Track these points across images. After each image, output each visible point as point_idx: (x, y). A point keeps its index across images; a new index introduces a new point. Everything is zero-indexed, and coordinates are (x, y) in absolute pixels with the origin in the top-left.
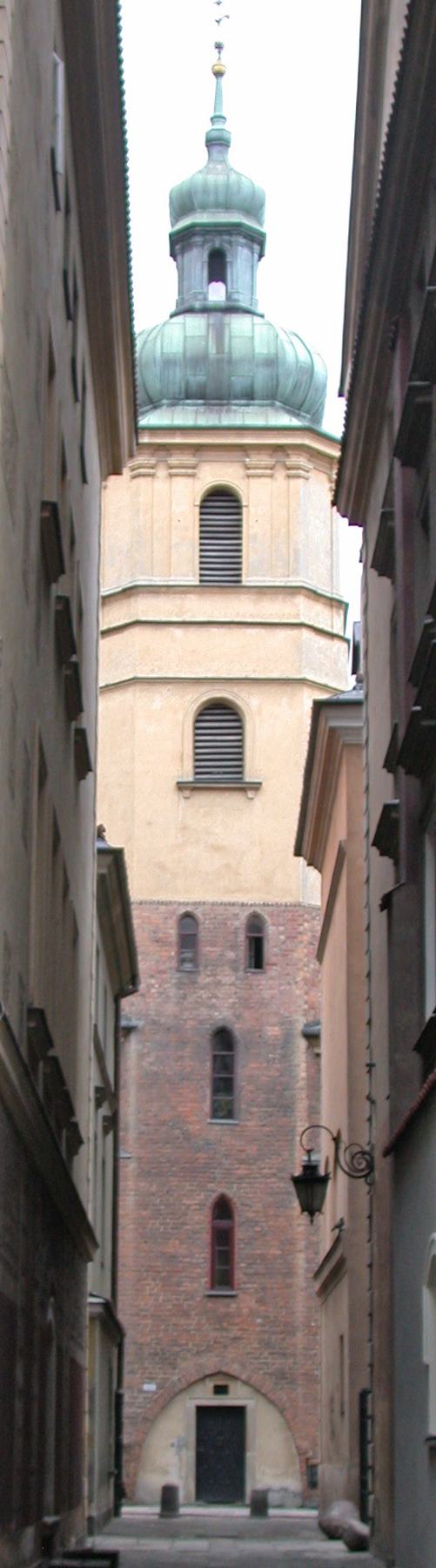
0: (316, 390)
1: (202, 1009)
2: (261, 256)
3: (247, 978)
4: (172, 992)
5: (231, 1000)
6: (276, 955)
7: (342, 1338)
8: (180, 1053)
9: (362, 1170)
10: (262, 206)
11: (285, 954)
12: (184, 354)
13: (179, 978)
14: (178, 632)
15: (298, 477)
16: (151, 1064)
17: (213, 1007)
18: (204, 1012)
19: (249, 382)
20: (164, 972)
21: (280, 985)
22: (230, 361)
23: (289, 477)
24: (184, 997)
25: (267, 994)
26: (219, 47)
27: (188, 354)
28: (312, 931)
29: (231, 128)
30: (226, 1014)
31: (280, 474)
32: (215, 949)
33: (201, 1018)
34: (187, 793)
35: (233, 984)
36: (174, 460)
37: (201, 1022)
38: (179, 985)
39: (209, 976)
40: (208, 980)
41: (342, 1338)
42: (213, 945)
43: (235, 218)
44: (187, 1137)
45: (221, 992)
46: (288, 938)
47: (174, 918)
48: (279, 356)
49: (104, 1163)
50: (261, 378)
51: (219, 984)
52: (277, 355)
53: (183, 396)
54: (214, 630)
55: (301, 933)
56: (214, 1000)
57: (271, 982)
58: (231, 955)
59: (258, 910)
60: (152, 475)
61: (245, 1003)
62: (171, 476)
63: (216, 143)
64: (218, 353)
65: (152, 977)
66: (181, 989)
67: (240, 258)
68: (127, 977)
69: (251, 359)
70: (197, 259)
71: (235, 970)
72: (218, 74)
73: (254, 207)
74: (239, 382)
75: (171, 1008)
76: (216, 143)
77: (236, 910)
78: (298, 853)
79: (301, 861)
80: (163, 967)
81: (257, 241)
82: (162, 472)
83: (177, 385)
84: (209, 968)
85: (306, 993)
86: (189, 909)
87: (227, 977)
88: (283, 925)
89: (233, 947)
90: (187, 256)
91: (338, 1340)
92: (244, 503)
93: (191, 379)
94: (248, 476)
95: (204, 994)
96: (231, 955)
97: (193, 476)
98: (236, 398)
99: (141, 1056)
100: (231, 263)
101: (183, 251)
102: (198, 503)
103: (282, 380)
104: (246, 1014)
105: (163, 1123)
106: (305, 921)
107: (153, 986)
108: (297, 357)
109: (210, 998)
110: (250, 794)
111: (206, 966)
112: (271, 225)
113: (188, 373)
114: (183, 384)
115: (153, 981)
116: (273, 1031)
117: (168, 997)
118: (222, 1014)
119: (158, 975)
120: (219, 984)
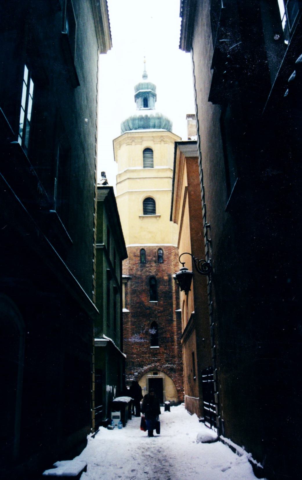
1: (147, 273)
2: (156, 101)
3: (158, 264)
4: (139, 269)
5: (155, 270)
6: (166, 258)
7: (193, 354)
8: (142, 285)
9: (206, 271)
10: (155, 89)
11: (168, 258)
13: (141, 265)
14: (138, 180)
15: (167, 143)
16: (134, 287)
17: (150, 272)
18: (148, 273)
20: (137, 264)
21: (167, 266)
23: (165, 143)
24: (142, 270)
25: (164, 268)
26: (145, 57)
28: (175, 252)
29: (148, 73)
30: (153, 274)
31: (163, 143)
32: (150, 257)
33: (147, 275)
34: (142, 219)
35: (155, 266)
36: (136, 141)
37: (147, 276)
38: (141, 267)
39: (148, 264)
40: (149, 265)
41: (193, 354)
42: (150, 256)
43: (150, 90)
44: (144, 306)
45: (152, 269)
46: (168, 254)
47: (139, 250)
51: (151, 266)
54: (147, 179)
55: (172, 253)
56: (150, 270)
57: (165, 265)
58: (154, 259)
59: (161, 247)
60: (131, 144)
61: (158, 271)
62: (136, 144)
65: (134, 265)
66: (141, 268)
67: (151, 101)
69: (154, 118)
70: (140, 101)
71: (155, 262)
72: (145, 63)
73: (154, 88)
75: (139, 273)
76: (145, 76)
77: (156, 247)
78: (171, 220)
79: (172, 222)
80: (137, 262)
81: (154, 95)
82: (133, 143)
84: (149, 262)
85: (174, 268)
86: (143, 247)
87: (154, 264)
88: (167, 251)
89: (155, 257)
93: (140, 123)
94: (154, 144)
95: (147, 269)
96: (154, 259)
97: (141, 144)
99: (131, 285)
103: (162, 122)
104: (159, 274)
105: (138, 303)
106: (173, 249)
107: (134, 267)
109: (149, 270)
110: (158, 218)
111: (148, 262)
112: (157, 92)
114: (138, 125)
115: (134, 266)
116: (166, 278)
117: (138, 270)
118: (153, 273)
119: (135, 265)
120: (151, 266)
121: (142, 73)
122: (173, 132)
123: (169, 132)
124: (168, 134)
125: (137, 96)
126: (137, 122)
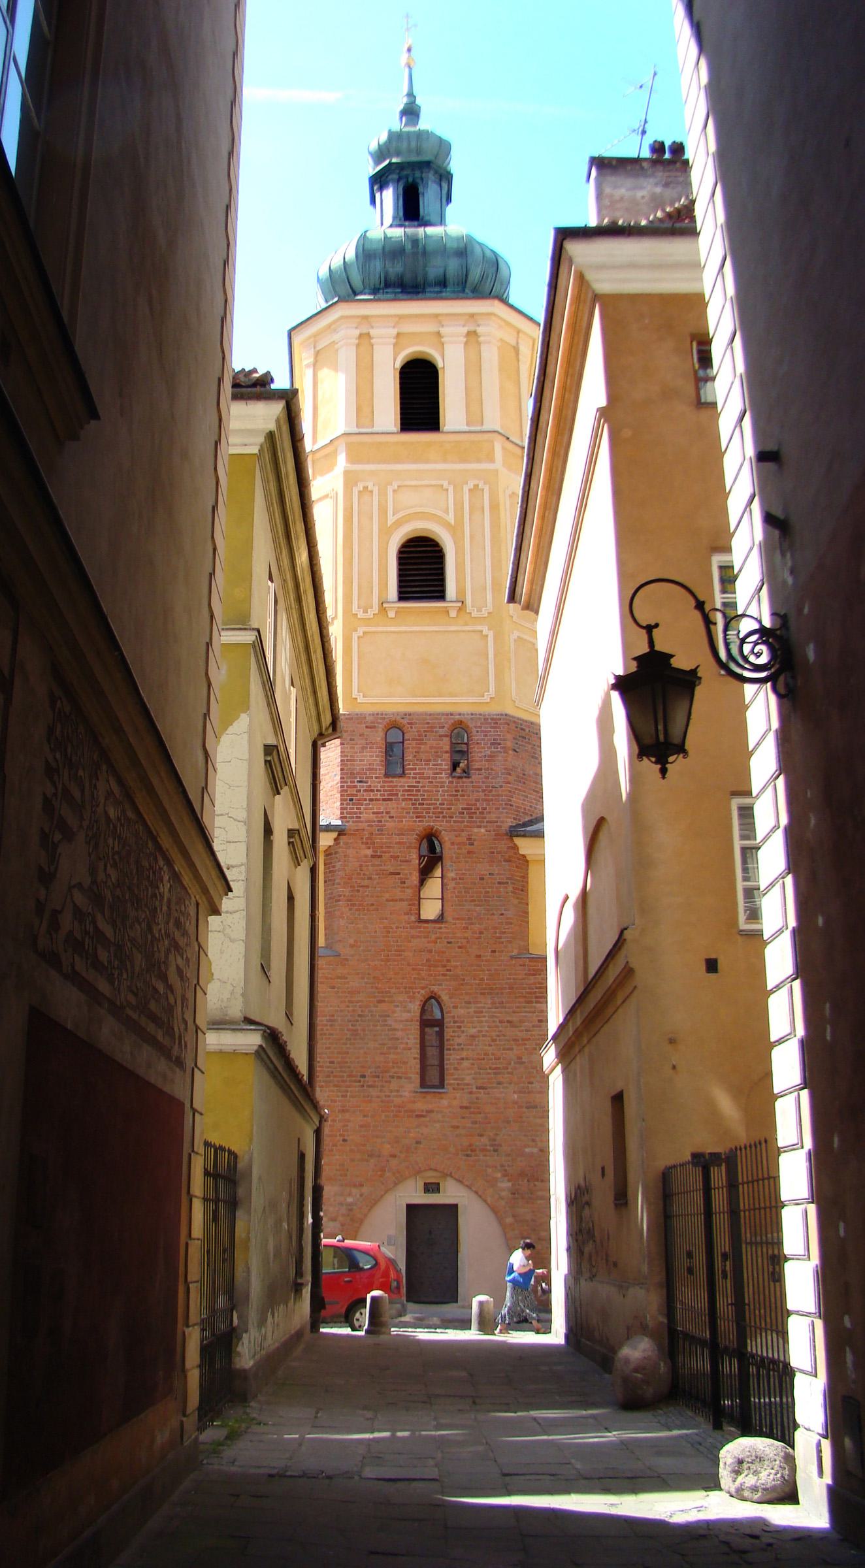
0: (502, 284)
2: (449, 199)
12: (384, 248)
19: (441, 271)
22: (425, 253)
27: (387, 249)
48: (468, 250)
49: (291, 898)
50: (453, 267)
52: (466, 248)
53: (383, 285)
63: (411, 112)
64: (413, 247)
68: (327, 719)
73: (444, 147)
74: (433, 272)
76: (411, 112)
78: (512, 598)
81: (445, 178)
83: (378, 276)
90: (385, 193)
91: (608, 1105)
92: (440, 365)
93: (391, 270)
98: (431, 285)
100: (423, 194)
101: (381, 189)
102: (398, 365)
108: (483, 253)
112: (456, 165)
113: (387, 266)
114: (383, 279)
121: (401, 102)
122: (511, 301)
123: (496, 302)
124: (495, 307)
125: (378, 181)
126: (377, 266)
